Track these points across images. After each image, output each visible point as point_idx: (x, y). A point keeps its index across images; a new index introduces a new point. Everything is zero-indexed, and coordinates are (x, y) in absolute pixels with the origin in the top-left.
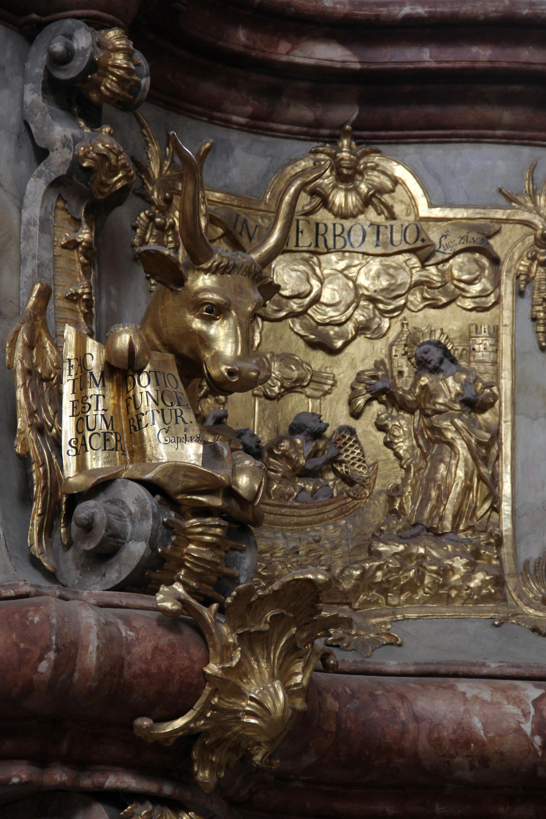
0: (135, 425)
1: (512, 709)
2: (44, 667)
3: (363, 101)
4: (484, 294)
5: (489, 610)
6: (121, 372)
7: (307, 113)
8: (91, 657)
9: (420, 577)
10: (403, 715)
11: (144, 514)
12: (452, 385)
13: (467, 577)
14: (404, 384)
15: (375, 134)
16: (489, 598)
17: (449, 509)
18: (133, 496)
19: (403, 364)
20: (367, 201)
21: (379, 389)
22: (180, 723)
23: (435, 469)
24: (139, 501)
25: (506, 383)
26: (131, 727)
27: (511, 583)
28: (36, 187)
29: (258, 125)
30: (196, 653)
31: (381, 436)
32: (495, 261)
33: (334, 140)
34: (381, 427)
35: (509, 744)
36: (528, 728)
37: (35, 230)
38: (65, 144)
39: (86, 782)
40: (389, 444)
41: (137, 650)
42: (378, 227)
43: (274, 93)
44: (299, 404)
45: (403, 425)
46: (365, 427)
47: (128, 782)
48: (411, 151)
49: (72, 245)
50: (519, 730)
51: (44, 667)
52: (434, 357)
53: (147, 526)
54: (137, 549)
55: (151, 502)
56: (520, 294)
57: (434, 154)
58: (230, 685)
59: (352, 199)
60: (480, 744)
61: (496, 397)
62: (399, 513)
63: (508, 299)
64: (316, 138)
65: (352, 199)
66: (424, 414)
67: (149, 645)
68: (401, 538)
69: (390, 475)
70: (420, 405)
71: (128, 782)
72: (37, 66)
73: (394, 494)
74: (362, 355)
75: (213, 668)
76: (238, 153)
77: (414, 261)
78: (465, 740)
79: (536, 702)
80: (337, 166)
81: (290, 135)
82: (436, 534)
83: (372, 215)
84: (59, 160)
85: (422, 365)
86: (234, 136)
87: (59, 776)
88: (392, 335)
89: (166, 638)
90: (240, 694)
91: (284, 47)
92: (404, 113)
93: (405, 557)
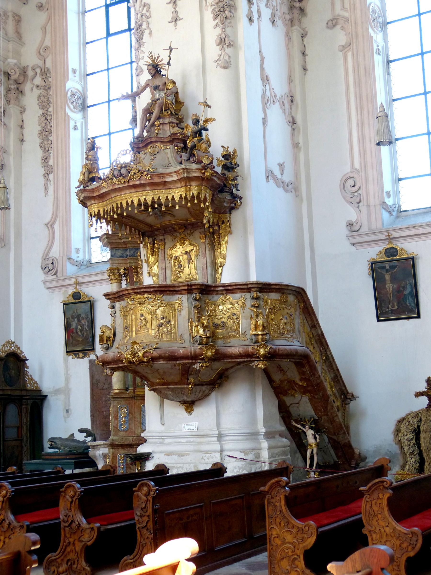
21: (229, 318)
29: (217, 294)
44: (222, 320)
45: (232, 321)
46: (228, 321)
57: (233, 295)
70: (233, 319)
73: (231, 328)
74: (228, 314)
78: (232, 353)
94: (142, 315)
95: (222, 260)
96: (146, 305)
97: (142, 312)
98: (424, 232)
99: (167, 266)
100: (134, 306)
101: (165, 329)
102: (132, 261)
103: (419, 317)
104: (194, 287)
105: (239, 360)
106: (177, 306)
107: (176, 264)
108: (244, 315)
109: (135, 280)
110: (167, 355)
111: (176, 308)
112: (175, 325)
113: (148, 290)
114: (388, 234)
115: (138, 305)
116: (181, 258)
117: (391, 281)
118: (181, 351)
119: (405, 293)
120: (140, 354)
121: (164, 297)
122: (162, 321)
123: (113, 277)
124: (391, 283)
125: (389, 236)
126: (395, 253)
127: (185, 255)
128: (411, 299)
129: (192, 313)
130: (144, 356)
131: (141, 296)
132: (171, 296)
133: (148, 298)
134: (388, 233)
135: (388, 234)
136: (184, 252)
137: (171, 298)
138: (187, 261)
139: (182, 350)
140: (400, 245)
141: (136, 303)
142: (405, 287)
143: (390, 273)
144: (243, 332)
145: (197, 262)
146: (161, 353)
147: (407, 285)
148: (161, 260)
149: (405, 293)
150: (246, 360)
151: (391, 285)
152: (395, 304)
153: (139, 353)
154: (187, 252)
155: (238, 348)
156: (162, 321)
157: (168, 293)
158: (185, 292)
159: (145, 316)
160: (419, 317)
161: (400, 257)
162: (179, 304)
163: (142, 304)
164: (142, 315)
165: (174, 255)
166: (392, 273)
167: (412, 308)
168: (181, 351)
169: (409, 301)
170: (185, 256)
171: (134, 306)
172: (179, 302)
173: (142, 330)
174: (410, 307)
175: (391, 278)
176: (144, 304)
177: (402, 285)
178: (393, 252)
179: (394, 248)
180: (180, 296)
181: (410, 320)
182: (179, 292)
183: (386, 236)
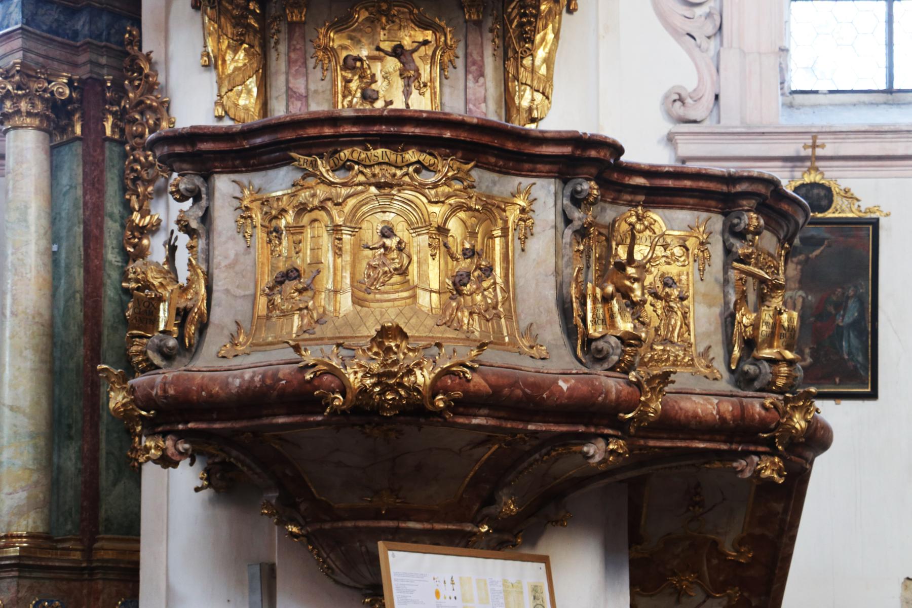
0: (612, 316)
1: (710, 407)
2: (600, 399)
3: (646, 195)
4: (684, 261)
5: (690, 369)
6: (607, 299)
7: (628, 197)
8: (613, 396)
9: (668, 358)
10: (677, 408)
11: (618, 347)
12: (675, 293)
13: (684, 358)
14: (659, 291)
15: (649, 204)
16: (690, 365)
17: (676, 334)
18: (613, 341)
19: (659, 284)
20: (646, 228)
22: (630, 415)
23: (670, 320)
24: (615, 343)
25: (691, 291)
26: (617, 415)
27: (696, 360)
28: (568, 232)
30: (638, 393)
31: (652, 308)
32: (687, 250)
33: (636, 206)
34: (652, 305)
35: (709, 418)
36: (715, 413)
37: (568, 246)
38: (579, 219)
39: (599, 432)
40: (655, 311)
41: (623, 393)
42: (650, 237)
43: (620, 191)
45: (660, 304)
47: (611, 432)
48: (660, 211)
49: (578, 251)
50: (712, 413)
51: (600, 399)
52: (668, 282)
53: (619, 351)
54: (615, 358)
55: (619, 342)
56: (695, 261)
57: (667, 212)
58: (646, 404)
59: (642, 227)
60: (700, 417)
61: (688, 297)
62: (660, 335)
63: (691, 263)
64: (630, 205)
65: (642, 227)
66: (666, 301)
67: (626, 391)
68: (662, 344)
69: (655, 322)
71: (611, 432)
72: (568, 191)
73: (657, 329)
75: (643, 399)
76: (608, 211)
77: (662, 249)
78: (696, 416)
79: (717, 404)
80: (637, 216)
81: (623, 205)
82: (672, 343)
83: (648, 233)
84: (577, 224)
85: (666, 285)
86: (607, 205)
87: (593, 430)
88: (655, 274)
89: (630, 389)
90: (649, 407)
91: (627, 179)
92: (659, 199)
93: (664, 350)
94: (388, 232)
95: (539, 97)
96: (408, 194)
97: (389, 217)
98: (891, 153)
99: (312, 87)
100: (351, 190)
101: (479, 298)
102: (103, 60)
103: (873, 395)
104: (593, 153)
105: (702, 445)
106: (513, 215)
107: (354, 85)
108: (702, 287)
109: (108, 132)
110: (519, 392)
111: (510, 224)
112: (506, 290)
113: (434, 132)
114: (814, 142)
115: (373, 189)
116: (377, 68)
117: (800, 282)
118: (564, 386)
119: (839, 321)
120: (423, 377)
121: (476, 174)
122: (465, 264)
123: (24, 106)
124: (800, 289)
125: (814, 146)
126: (824, 203)
127: (389, 59)
128: (854, 341)
129: (568, 252)
130: (435, 388)
131: (392, 156)
132: (495, 176)
133: (421, 167)
134: (814, 138)
135: (814, 142)
136: (387, 46)
137: (494, 183)
138: (399, 83)
139: (565, 381)
140: (839, 178)
141: (361, 178)
142: (841, 306)
143: (802, 257)
144: (701, 349)
145: (447, 91)
146: (501, 382)
147: (848, 298)
148: (290, 62)
149: (839, 321)
150: (724, 447)
151: (800, 293)
152: (807, 351)
153: (418, 372)
154: (400, 46)
155: (715, 401)
156: (465, 264)
157: (492, 160)
158: (547, 168)
159: (399, 234)
160: (873, 395)
161: (837, 215)
162: (523, 211)
163: (391, 186)
164: (388, 232)
165: (344, 54)
166: (808, 259)
167: (855, 367)
168: (561, 383)
169: (849, 346)
170: (393, 64)
171: (351, 190)
172: (523, 204)
173: (387, 288)
174: (851, 364)
175: (802, 271)
176: (401, 186)
177: (834, 298)
178: (819, 198)
179: (822, 186)
180: (525, 182)
181: (846, 404)
182: (527, 166)
183: (805, 147)
